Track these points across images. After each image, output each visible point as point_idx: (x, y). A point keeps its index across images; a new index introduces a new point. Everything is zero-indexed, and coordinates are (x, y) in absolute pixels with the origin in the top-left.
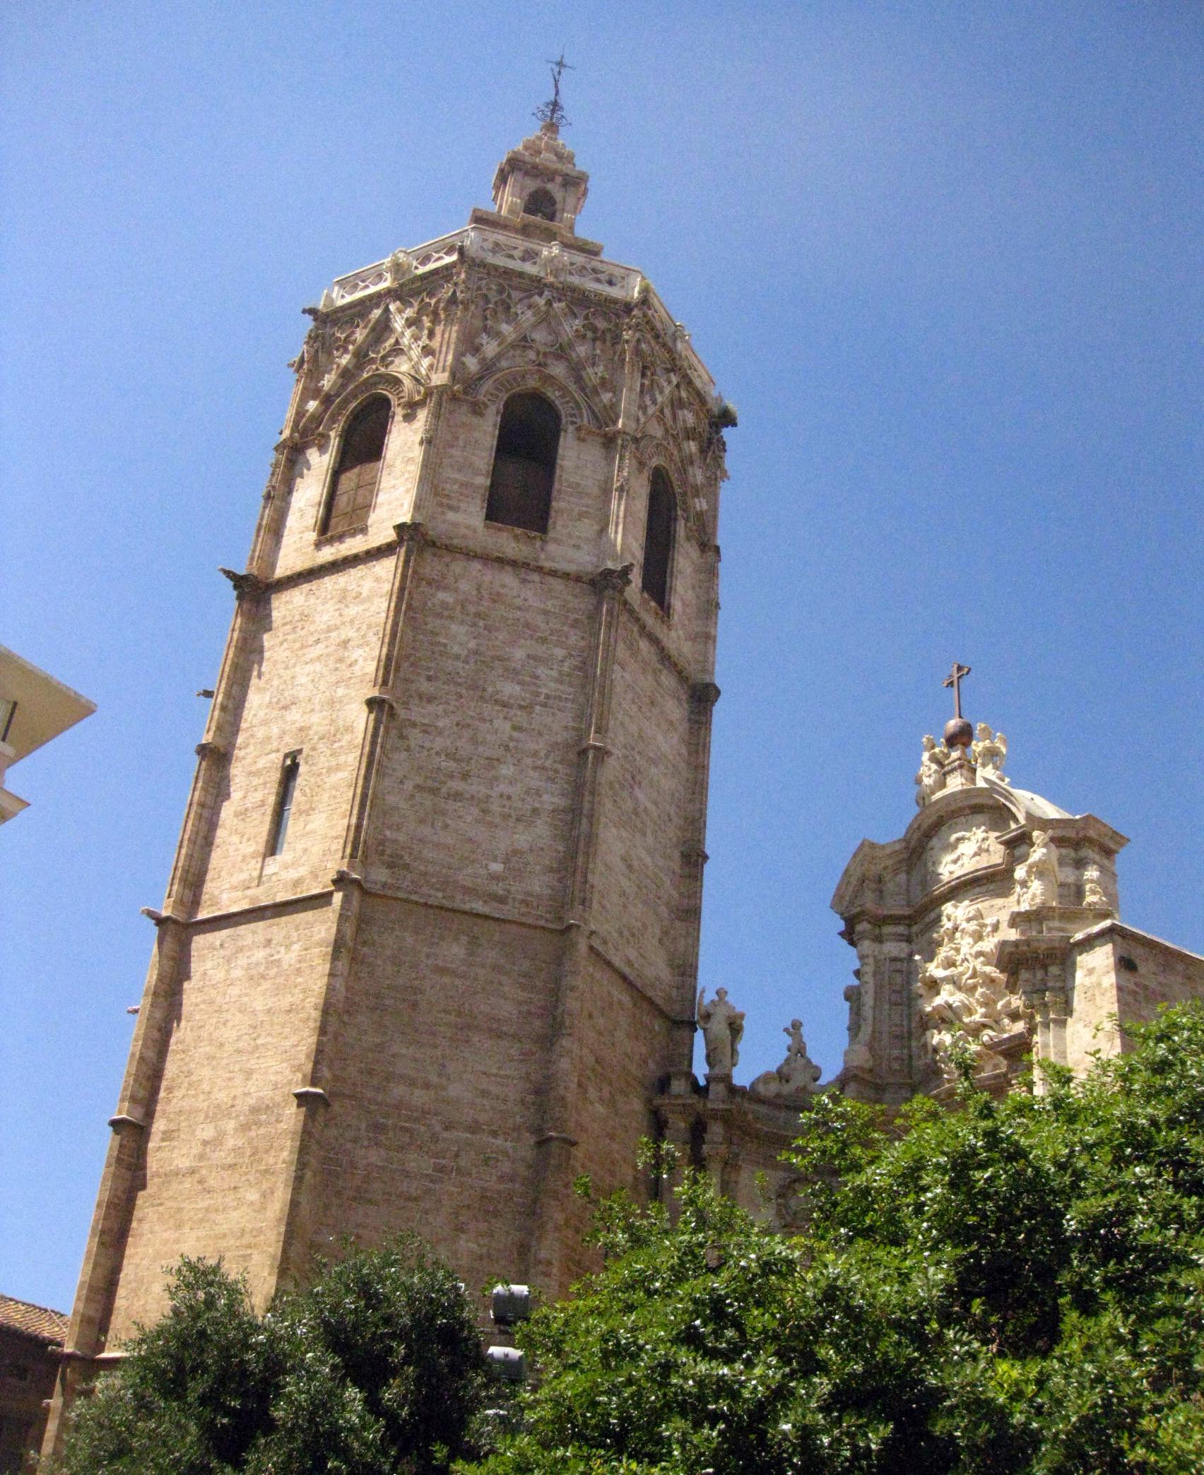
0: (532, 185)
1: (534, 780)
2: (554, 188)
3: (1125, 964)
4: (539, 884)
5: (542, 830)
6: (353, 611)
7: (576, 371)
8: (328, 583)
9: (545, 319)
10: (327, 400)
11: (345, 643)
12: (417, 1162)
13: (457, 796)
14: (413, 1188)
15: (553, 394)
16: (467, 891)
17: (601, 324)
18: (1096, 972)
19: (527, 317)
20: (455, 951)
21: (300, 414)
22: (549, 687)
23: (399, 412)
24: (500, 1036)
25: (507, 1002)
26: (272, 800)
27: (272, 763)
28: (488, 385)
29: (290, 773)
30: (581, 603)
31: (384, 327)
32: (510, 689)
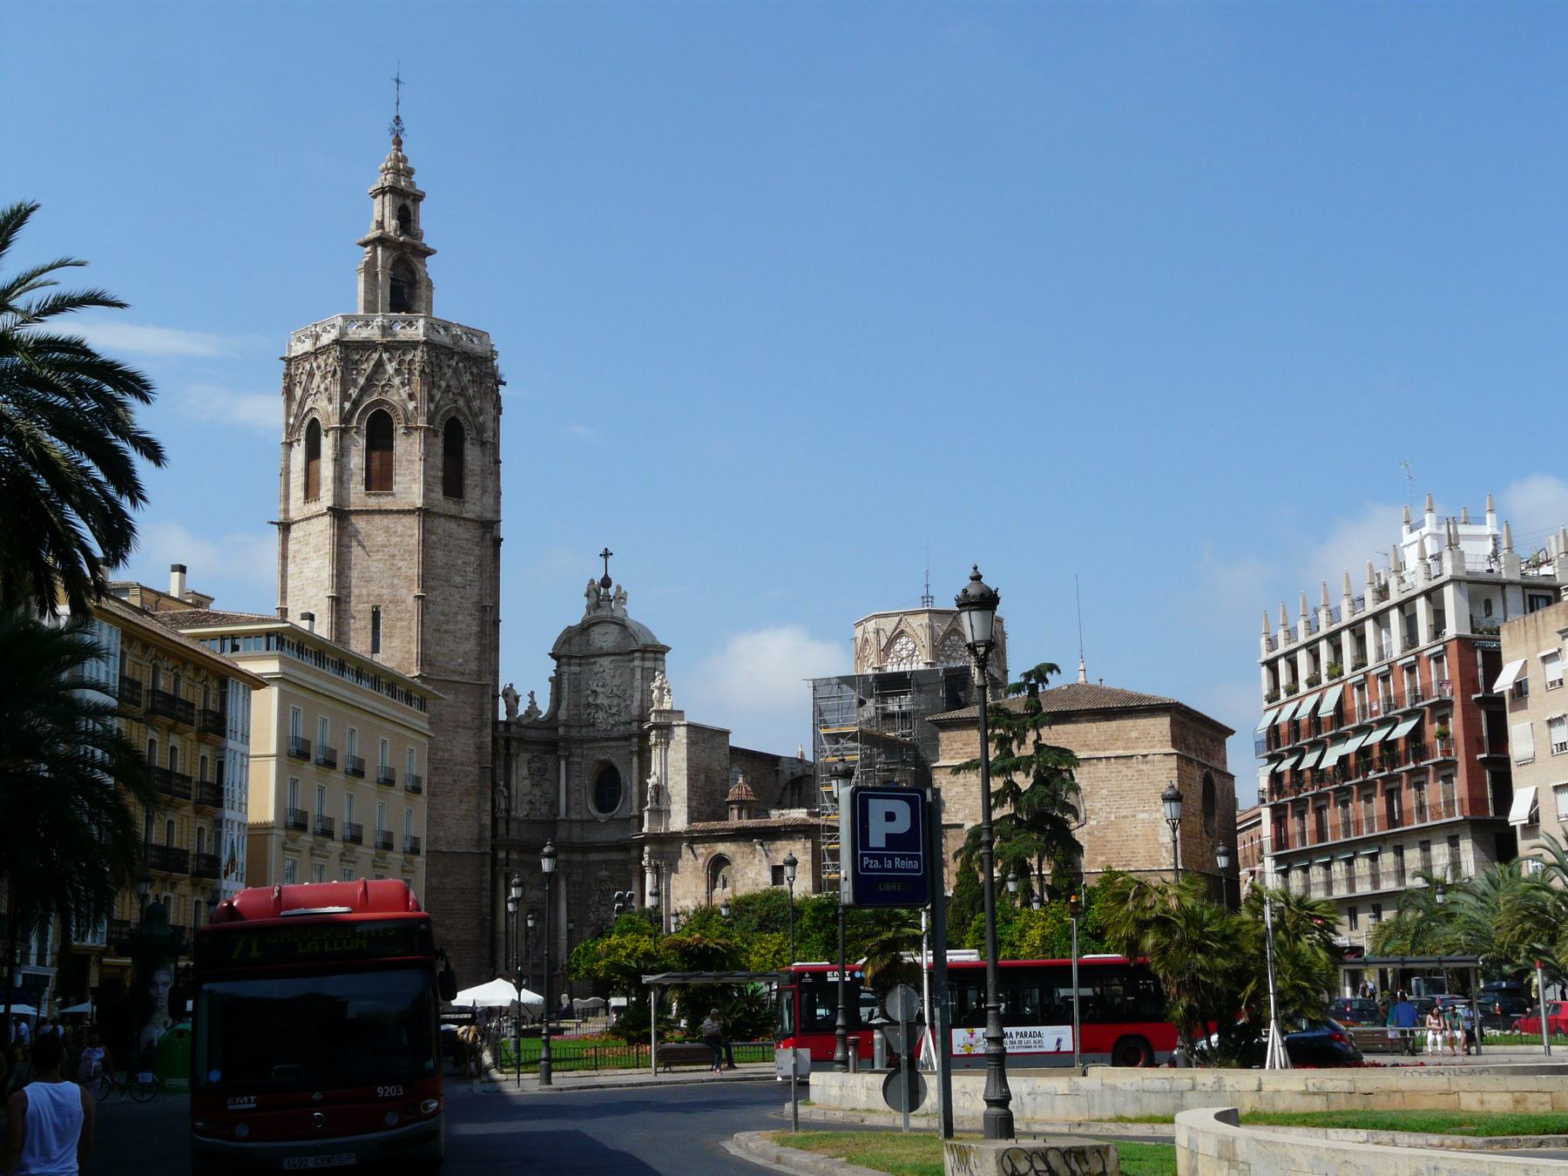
0: (400, 202)
1: (469, 620)
2: (409, 202)
3: (689, 732)
4: (473, 665)
5: (473, 641)
6: (394, 540)
7: (468, 402)
8: (377, 519)
9: (456, 371)
10: (356, 404)
11: (394, 556)
12: (449, 780)
13: (446, 632)
14: (447, 789)
15: (461, 419)
16: (454, 672)
17: (475, 370)
18: (680, 734)
19: (450, 373)
20: (450, 698)
21: (342, 408)
22: (471, 576)
23: (399, 430)
24: (465, 728)
25: (467, 715)
26: (370, 626)
27: (368, 607)
28: (438, 420)
29: (376, 616)
30: (478, 533)
31: (379, 364)
32: (458, 579)
